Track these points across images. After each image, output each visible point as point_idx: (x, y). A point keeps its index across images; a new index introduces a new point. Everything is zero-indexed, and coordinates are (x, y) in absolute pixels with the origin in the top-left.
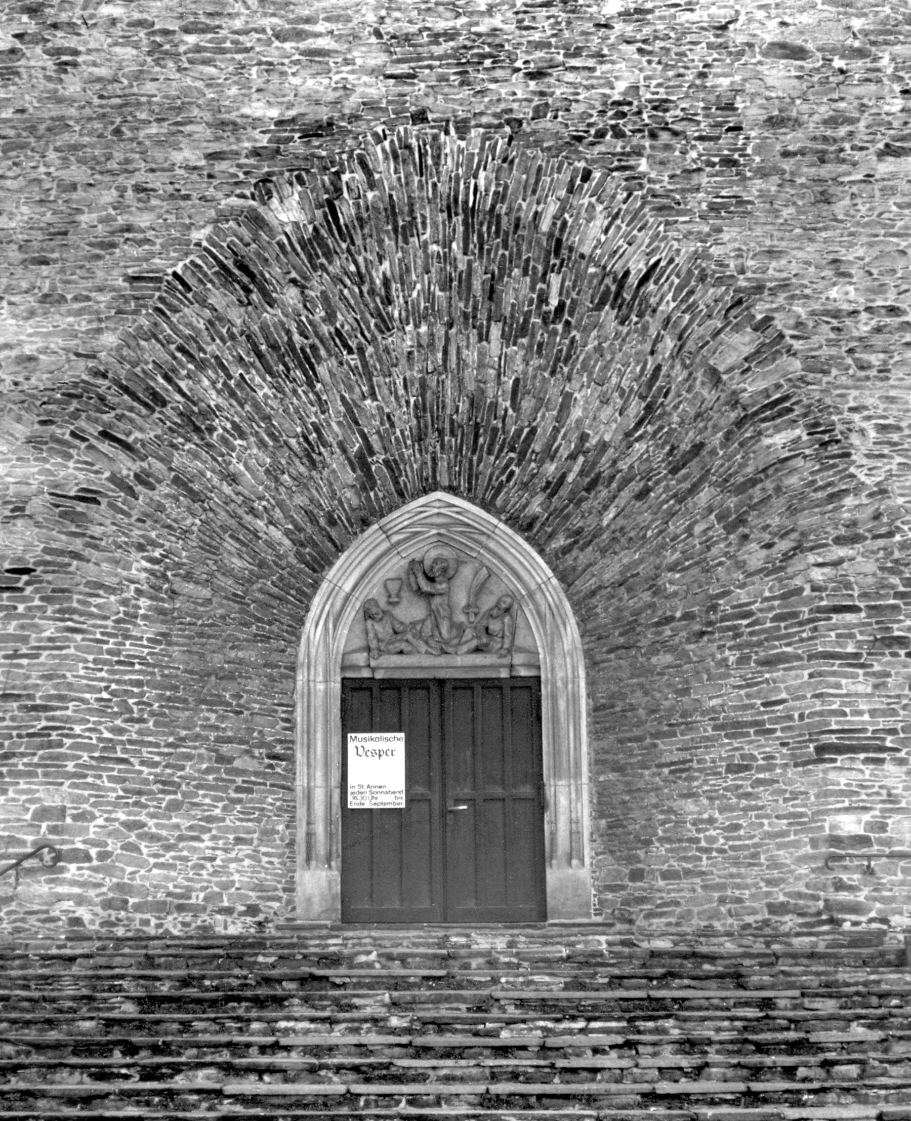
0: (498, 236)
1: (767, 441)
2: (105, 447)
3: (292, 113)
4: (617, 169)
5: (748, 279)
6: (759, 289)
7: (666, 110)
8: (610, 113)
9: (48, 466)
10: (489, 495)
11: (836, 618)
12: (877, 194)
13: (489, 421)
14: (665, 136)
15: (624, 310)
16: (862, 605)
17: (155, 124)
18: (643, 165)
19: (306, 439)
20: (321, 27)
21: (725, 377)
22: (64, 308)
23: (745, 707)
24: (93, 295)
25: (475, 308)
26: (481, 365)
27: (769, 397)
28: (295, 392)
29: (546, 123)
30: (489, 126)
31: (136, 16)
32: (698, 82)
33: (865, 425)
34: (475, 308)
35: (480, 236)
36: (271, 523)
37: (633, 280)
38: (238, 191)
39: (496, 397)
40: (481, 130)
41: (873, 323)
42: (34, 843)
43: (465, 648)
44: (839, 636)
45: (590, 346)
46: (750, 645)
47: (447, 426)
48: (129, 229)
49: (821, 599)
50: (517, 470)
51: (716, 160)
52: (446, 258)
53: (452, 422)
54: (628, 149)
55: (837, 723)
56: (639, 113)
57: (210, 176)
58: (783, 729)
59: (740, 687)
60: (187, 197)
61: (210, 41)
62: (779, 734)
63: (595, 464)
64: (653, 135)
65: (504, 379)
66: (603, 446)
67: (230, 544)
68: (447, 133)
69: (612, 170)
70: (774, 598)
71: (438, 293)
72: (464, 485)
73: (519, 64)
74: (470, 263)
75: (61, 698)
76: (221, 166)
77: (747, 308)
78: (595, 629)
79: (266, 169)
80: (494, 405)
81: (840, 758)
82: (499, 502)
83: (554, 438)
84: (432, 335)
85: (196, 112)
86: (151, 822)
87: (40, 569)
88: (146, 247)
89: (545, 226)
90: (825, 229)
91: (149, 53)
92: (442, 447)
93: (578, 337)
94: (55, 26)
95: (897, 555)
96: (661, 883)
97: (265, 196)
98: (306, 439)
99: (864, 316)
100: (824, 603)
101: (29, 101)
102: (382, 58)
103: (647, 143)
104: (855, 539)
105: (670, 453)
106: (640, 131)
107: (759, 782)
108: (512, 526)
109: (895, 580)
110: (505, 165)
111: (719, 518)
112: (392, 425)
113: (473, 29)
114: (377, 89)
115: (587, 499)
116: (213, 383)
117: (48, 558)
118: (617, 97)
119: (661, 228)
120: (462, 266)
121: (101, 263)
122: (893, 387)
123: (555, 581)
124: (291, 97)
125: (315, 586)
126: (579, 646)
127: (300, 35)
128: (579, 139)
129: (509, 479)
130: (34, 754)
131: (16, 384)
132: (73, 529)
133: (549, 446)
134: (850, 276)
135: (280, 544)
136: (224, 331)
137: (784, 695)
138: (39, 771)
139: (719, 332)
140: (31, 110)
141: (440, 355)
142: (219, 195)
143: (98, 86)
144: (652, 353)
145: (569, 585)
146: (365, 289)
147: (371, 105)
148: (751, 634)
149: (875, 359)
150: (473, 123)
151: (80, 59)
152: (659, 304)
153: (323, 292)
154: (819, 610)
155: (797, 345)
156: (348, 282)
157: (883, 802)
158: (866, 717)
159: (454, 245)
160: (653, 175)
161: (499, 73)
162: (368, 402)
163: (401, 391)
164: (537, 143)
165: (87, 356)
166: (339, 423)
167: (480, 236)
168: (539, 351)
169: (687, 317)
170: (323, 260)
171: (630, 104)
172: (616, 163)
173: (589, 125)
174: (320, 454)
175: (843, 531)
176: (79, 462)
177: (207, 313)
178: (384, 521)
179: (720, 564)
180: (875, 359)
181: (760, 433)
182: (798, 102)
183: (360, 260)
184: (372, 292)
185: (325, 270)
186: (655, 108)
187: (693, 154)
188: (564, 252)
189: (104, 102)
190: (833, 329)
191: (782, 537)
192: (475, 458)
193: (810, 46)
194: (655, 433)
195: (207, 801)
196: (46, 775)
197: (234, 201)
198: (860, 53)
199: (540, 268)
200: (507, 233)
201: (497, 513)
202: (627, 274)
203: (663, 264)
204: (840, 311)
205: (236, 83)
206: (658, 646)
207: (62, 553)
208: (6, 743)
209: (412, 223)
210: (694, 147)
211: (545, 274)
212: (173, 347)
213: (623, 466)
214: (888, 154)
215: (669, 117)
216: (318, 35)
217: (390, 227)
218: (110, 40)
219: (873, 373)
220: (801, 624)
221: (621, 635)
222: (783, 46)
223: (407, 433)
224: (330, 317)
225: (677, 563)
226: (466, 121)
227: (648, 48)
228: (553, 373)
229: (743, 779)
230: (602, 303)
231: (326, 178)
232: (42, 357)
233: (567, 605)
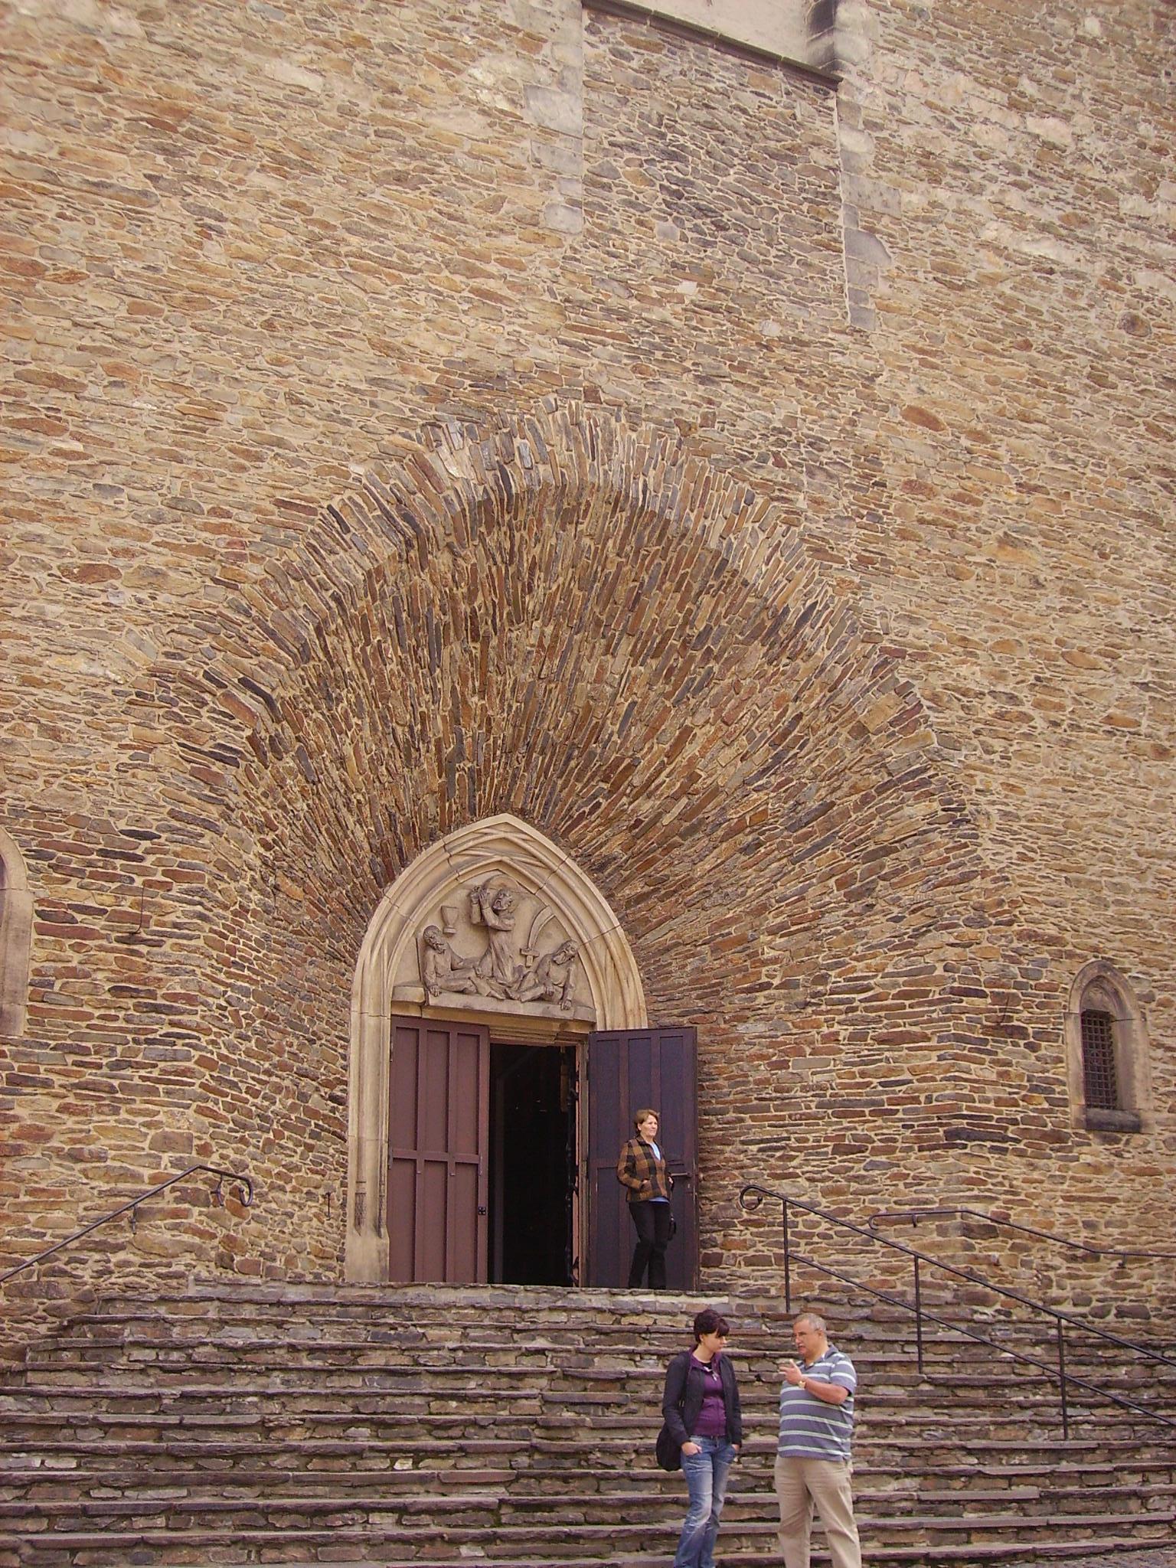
0: (659, 543)
1: (907, 811)
2: (246, 698)
3: (461, 355)
4: (778, 499)
5: (892, 641)
6: (901, 654)
7: (821, 450)
8: (772, 439)
9: (175, 710)
11: (967, 1002)
12: (998, 580)
14: (820, 478)
15: (776, 649)
16: (987, 990)
17: (311, 328)
18: (802, 502)
19: (411, 728)
20: (493, 268)
21: (874, 738)
22: (199, 520)
23: (859, 1085)
24: (235, 511)
25: (611, 616)
26: (599, 679)
27: (910, 765)
28: (416, 673)
29: (712, 433)
30: (659, 422)
31: (293, 197)
32: (848, 428)
33: (991, 809)
34: (611, 616)
35: (640, 538)
36: (358, 821)
37: (792, 618)
38: (403, 430)
39: (605, 719)
40: (653, 426)
41: (996, 707)
42: (154, 1179)
43: (529, 995)
44: (969, 1020)
45: (727, 681)
46: (865, 1021)
48: (280, 443)
49: (954, 980)
50: (604, 804)
51: (865, 512)
52: (600, 556)
54: (787, 481)
55: (968, 1108)
56: (797, 445)
57: (372, 404)
58: (905, 1111)
59: (853, 1064)
60: (347, 422)
61: (375, 249)
62: (900, 1115)
63: (701, 807)
64: (811, 474)
65: (619, 700)
66: (715, 792)
67: (324, 840)
68: (618, 420)
69: (773, 499)
70: (899, 975)
71: (576, 591)
72: (538, 810)
73: (688, 364)
74: (620, 566)
75: (190, 999)
76: (383, 396)
77: (892, 671)
78: (665, 989)
79: (433, 412)
80: (599, 728)
81: (970, 1144)
82: (573, 836)
83: (658, 773)
84: (555, 637)
85: (357, 325)
86: (252, 1164)
87: (164, 836)
88: (299, 469)
89: (713, 544)
90: (956, 603)
91: (308, 243)
92: (528, 763)
93: (716, 669)
94: (196, 179)
95: (1016, 944)
96: (745, 1270)
97: (433, 445)
98: (411, 728)
99: (989, 699)
100: (956, 985)
101: (161, 259)
102: (555, 322)
103: (804, 478)
104: (982, 924)
105: (794, 809)
106: (800, 465)
107: (874, 1165)
108: (581, 865)
109: (1015, 969)
110: (674, 469)
111: (840, 885)
112: (489, 731)
113: (644, 315)
114: (551, 354)
115: (681, 845)
116: (354, 646)
117: (177, 824)
118: (779, 425)
119: (817, 570)
120: (612, 569)
121: (245, 475)
122: (1013, 775)
123: (620, 931)
124: (461, 338)
125: (376, 902)
126: (643, 1005)
127: (472, 272)
128: (744, 459)
129: (591, 813)
130: (155, 1066)
131: (140, 602)
132: (207, 792)
133: (651, 781)
134: (976, 656)
135: (362, 848)
136: (377, 587)
137: (907, 1076)
138: (161, 1087)
139: (868, 690)
140: (165, 270)
141: (557, 662)
142: (382, 428)
143: (247, 265)
144: (796, 699)
146: (511, 570)
147: (543, 369)
148: (866, 1009)
149: (998, 745)
150: (644, 416)
151: (227, 227)
152: (816, 649)
153: (474, 565)
154: (953, 991)
155: (933, 717)
156: (499, 559)
157: (1006, 1192)
158: (991, 1106)
159: (610, 543)
160: (810, 514)
161: (669, 368)
162: (475, 699)
163: (508, 695)
164: (705, 454)
165: (228, 586)
166: (444, 718)
167: (640, 538)
168: (667, 677)
169: (840, 668)
170: (483, 529)
171: (790, 434)
172: (777, 493)
173: (752, 446)
174: (418, 750)
175: (972, 913)
176: (214, 711)
177: (367, 564)
178: (449, 838)
179: (836, 933)
180: (998, 745)
181: (903, 801)
182: (933, 471)
183: (517, 535)
184: (518, 575)
185: (483, 541)
186: (811, 444)
187: (845, 501)
188: (726, 576)
189: (254, 286)
190: (963, 707)
191: (914, 912)
192: (560, 782)
193: (941, 417)
194: (780, 785)
195: (290, 1145)
196: (168, 1093)
197: (398, 439)
198: (979, 437)
199: (696, 587)
200: (670, 542)
201: (568, 847)
202: (786, 611)
203: (819, 608)
204: (968, 689)
205: (402, 304)
206: (748, 1013)
207: (193, 820)
208: (119, 1049)
209: (576, 509)
210: (844, 494)
211: (699, 594)
212: (327, 595)
213: (733, 816)
214: (1007, 543)
215: (823, 457)
216: (490, 276)
217: (554, 508)
218: (262, 215)
219: (996, 757)
220: (931, 1003)
221: (699, 998)
222: (921, 412)
223: (500, 742)
224: (471, 596)
225: (782, 926)
226: (637, 411)
227: (806, 380)
228: (677, 702)
229: (856, 1161)
230: (753, 637)
231: (497, 438)
232: (171, 573)
233: (633, 960)
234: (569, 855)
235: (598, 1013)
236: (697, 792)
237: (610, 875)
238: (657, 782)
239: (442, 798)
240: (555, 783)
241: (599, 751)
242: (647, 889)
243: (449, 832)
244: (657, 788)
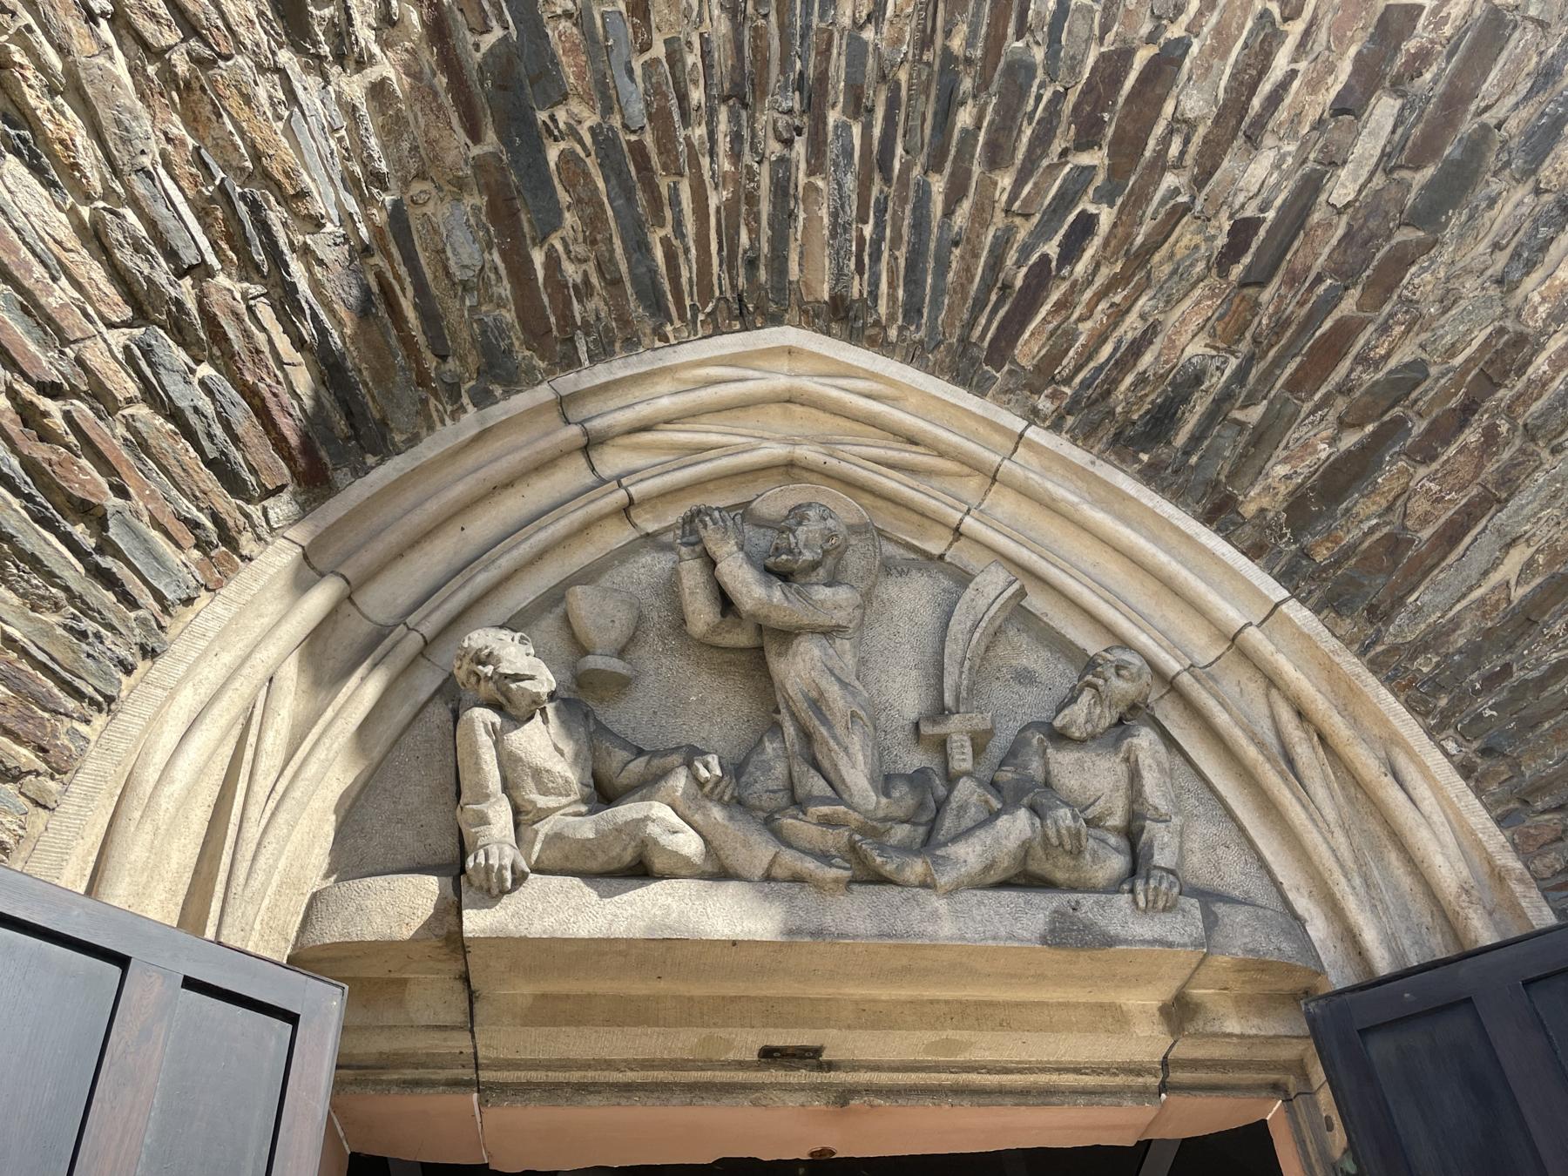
10: (986, 329)
13: (996, 41)
47: (838, 66)
50: (1106, 217)
53: (857, 50)
63: (1455, 99)
82: (1029, 348)
83: (1260, 55)
123: (1299, 614)
129: (1071, 251)
133: (1244, 84)
145: (1379, 615)
178: (568, 382)
192: (938, 185)
223: (692, 59)
234: (1033, 416)
235: (1318, 929)
236: (1423, 57)
237: (1196, 439)
238: (1266, 87)
239: (502, 213)
240: (924, 192)
241: (1039, 54)
242: (1350, 440)
243: (570, 362)
244: (1275, 99)
